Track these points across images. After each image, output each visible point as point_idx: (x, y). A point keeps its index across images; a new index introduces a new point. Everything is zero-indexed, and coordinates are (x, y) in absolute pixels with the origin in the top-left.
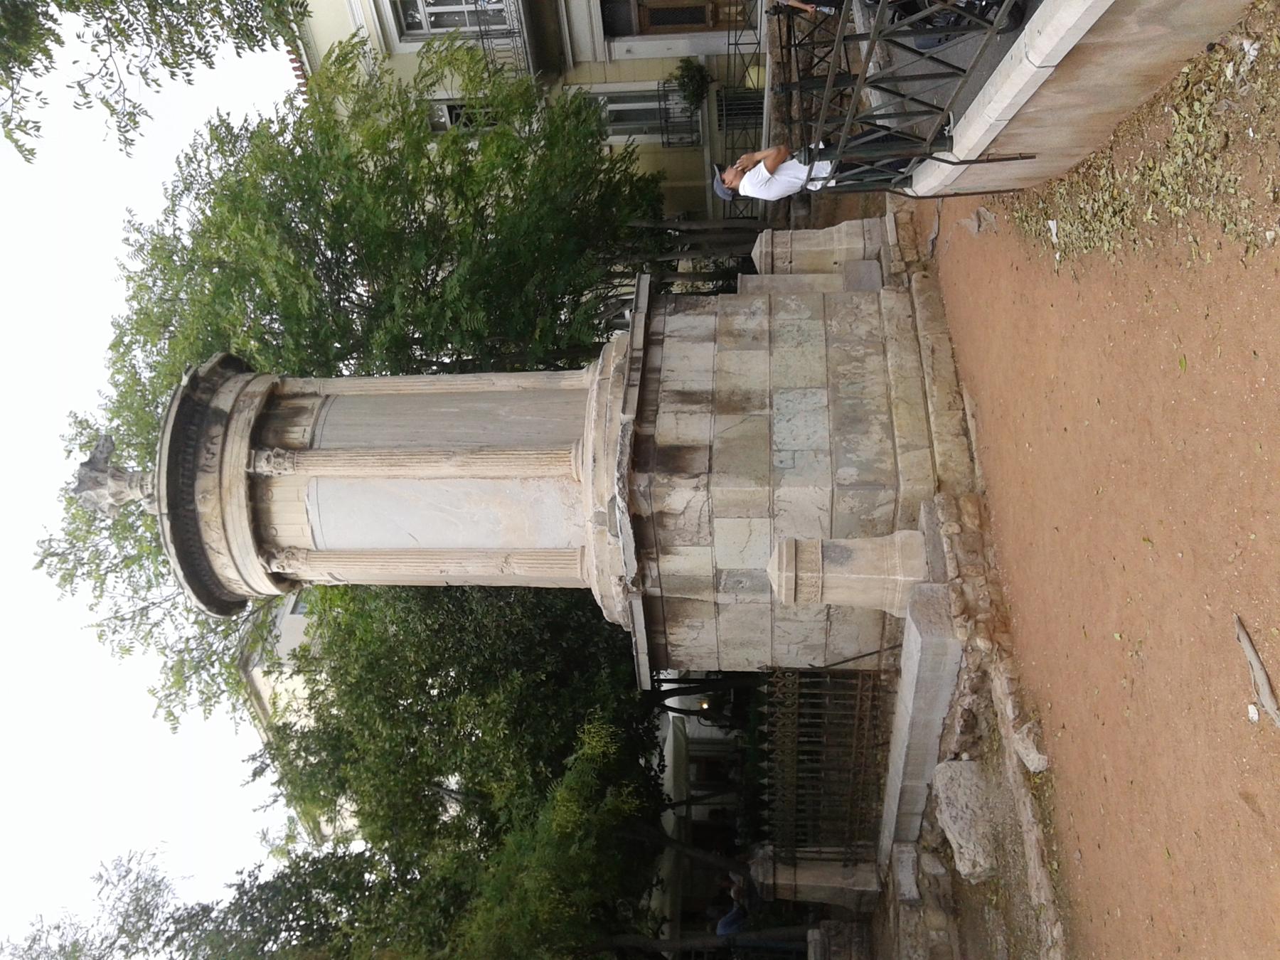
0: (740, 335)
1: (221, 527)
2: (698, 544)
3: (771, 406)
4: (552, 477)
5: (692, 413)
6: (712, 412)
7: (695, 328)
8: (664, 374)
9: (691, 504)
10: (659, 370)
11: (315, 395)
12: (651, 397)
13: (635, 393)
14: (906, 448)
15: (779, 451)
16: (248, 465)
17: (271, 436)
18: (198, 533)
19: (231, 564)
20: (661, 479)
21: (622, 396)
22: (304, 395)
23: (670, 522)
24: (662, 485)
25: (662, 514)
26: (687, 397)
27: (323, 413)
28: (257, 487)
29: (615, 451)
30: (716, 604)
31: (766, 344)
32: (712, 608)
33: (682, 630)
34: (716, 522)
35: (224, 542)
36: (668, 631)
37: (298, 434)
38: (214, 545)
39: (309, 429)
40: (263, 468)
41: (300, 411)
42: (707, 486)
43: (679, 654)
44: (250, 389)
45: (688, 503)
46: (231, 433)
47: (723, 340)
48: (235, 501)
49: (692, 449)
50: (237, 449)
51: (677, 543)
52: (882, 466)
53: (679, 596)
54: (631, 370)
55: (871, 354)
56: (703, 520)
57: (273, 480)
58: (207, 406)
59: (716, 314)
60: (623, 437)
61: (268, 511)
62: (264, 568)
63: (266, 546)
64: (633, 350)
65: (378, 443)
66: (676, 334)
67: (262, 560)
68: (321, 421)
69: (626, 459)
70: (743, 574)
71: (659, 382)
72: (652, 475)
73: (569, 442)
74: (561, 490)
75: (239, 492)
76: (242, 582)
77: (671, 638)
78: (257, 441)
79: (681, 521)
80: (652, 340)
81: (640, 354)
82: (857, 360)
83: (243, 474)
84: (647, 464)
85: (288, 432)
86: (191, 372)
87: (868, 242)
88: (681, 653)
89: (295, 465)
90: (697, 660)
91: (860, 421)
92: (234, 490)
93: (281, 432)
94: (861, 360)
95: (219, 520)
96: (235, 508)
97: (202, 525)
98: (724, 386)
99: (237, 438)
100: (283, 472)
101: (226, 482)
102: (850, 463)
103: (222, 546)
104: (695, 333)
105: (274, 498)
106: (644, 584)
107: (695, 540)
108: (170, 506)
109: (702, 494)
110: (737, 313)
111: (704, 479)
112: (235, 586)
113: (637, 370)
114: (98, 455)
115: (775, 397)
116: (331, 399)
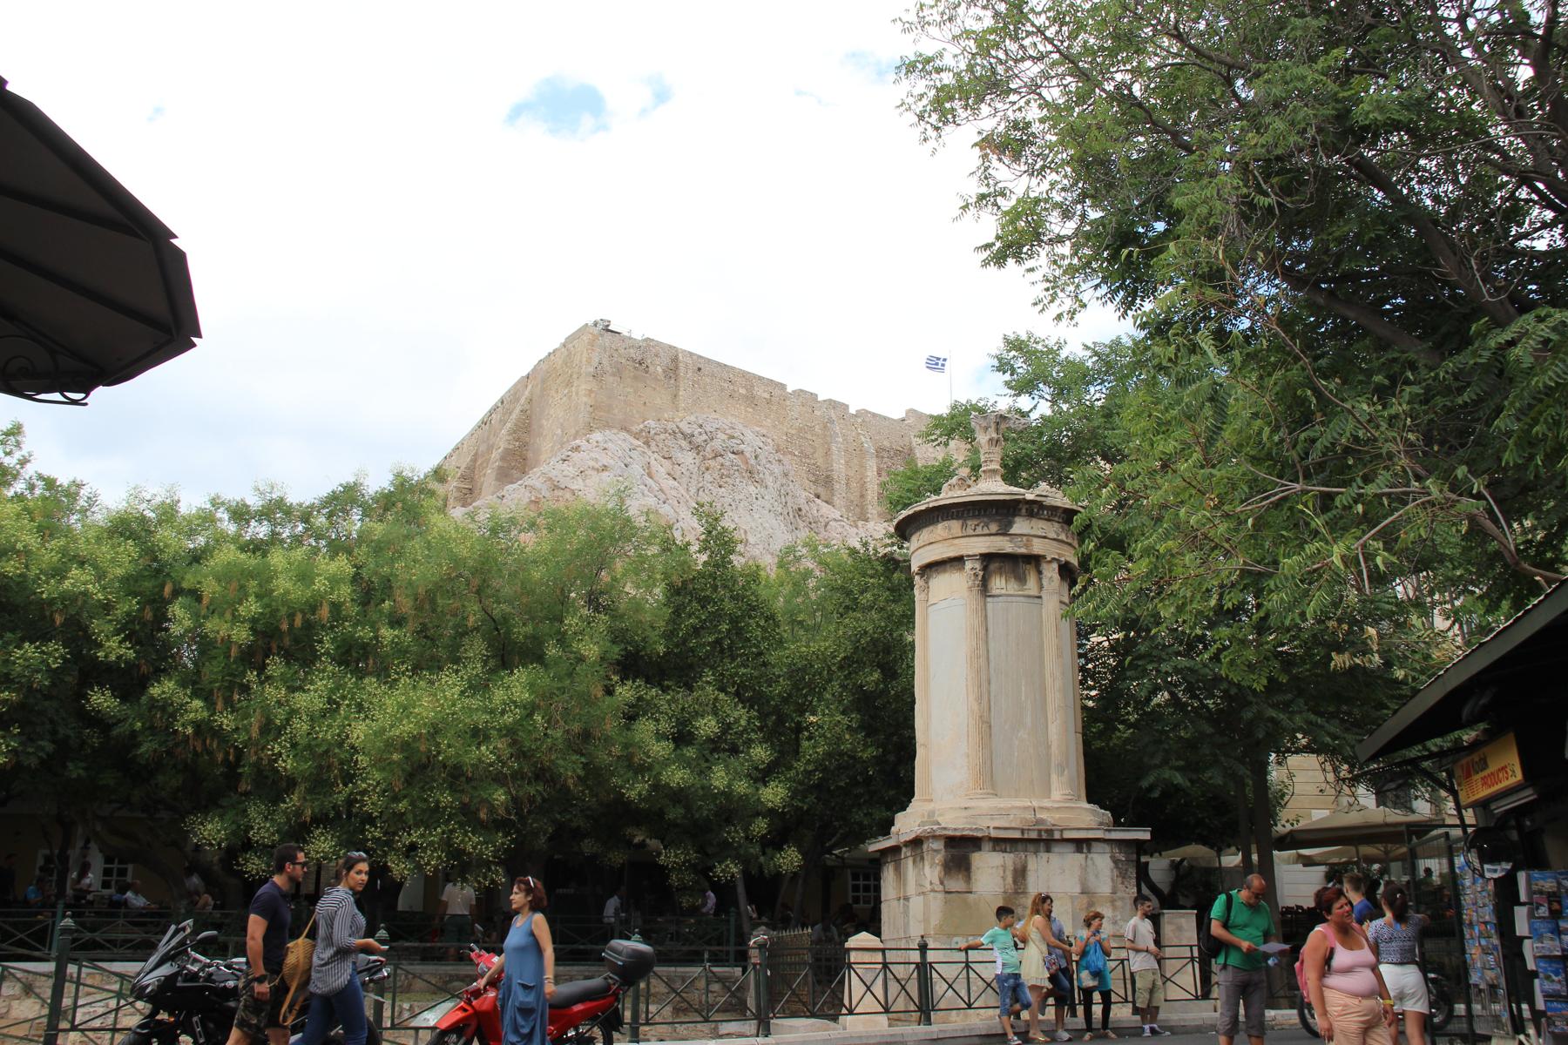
5: (1004, 878)
7: (1097, 876)
8: (1044, 856)
10: (1048, 850)
11: (1041, 587)
12: (1020, 846)
13: (1017, 835)
17: (997, 565)
20: (939, 858)
21: (1013, 825)
22: (1040, 579)
24: (933, 859)
25: (922, 859)
26: (1020, 874)
27: (1022, 599)
37: (998, 584)
39: (1003, 592)
40: (969, 565)
41: (1022, 580)
42: (933, 891)
44: (1035, 540)
47: (1085, 899)
49: (968, 878)
54: (1040, 831)
58: (1014, 515)
60: (971, 829)
61: (945, 571)
64: (1062, 831)
65: (992, 645)
66: (1089, 862)
68: (1010, 599)
69: (951, 833)
71: (1036, 852)
72: (943, 852)
73: (993, 786)
75: (951, 553)
78: (987, 558)
80: (1081, 845)
81: (1057, 836)
84: (952, 847)
86: (1039, 499)
89: (970, 588)
93: (1000, 571)
97: (931, 528)
101: (956, 541)
103: (921, 543)
104: (1091, 878)
108: (935, 508)
109: (929, 887)
111: (941, 888)
113: (1040, 835)
116: (1037, 601)
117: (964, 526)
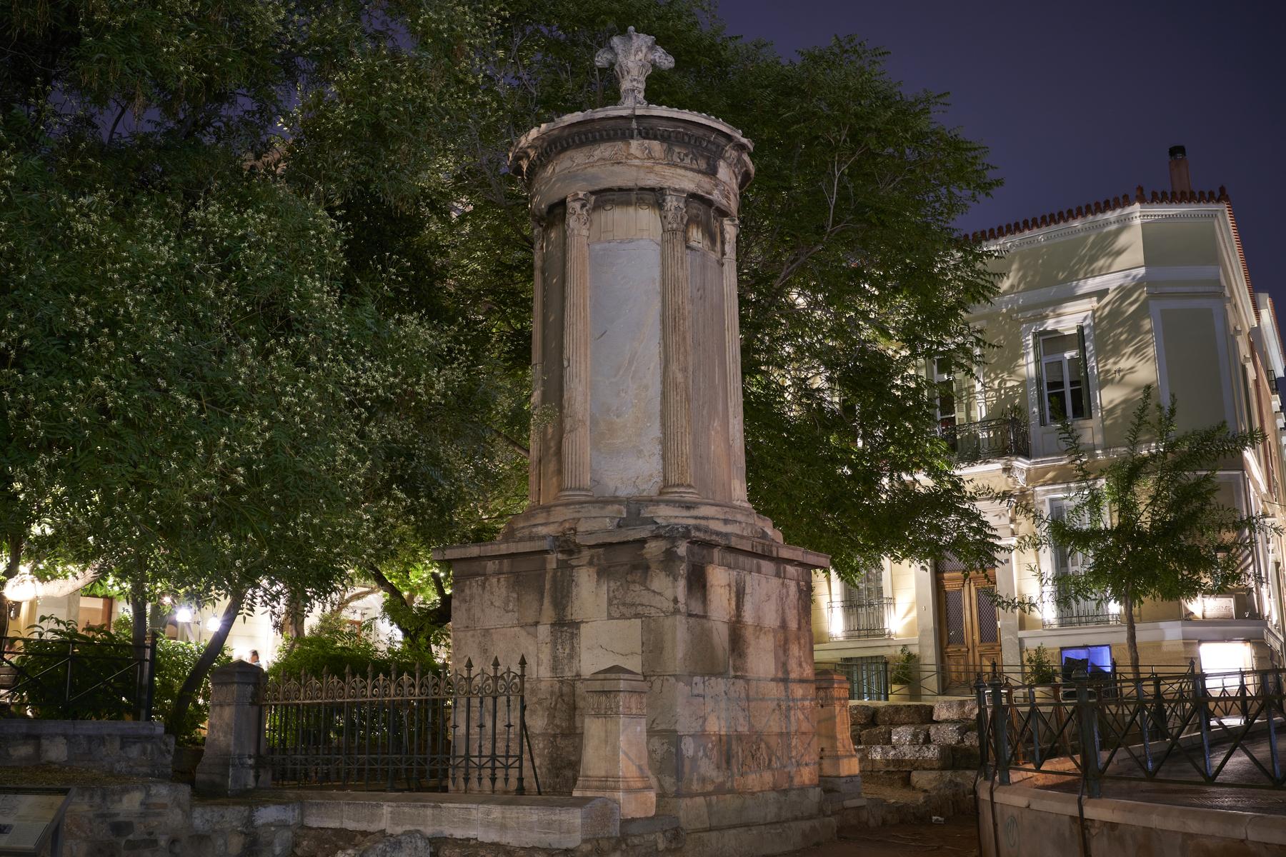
0: (786, 651)
2: (610, 603)
3: (736, 677)
4: (664, 468)
6: (730, 619)
9: (658, 598)
11: (723, 254)
12: (741, 559)
14: (709, 805)
15: (704, 682)
16: (675, 190)
18: (609, 139)
20: (683, 569)
23: (638, 575)
25: (648, 568)
26: (740, 595)
28: (654, 197)
29: (697, 528)
30: (536, 624)
31: (780, 675)
32: (530, 621)
33: (503, 590)
34: (638, 621)
36: (502, 578)
37: (696, 235)
38: (596, 153)
39: (700, 245)
40: (671, 202)
41: (713, 241)
43: (473, 588)
45: (660, 594)
47: (781, 636)
49: (704, 600)
50: (688, 181)
51: (612, 584)
52: (695, 782)
53: (547, 586)
55: (774, 775)
56: (640, 608)
57: (657, 212)
59: (799, 628)
61: (628, 203)
63: (593, 198)
67: (581, 195)
70: (573, 648)
74: (651, 475)
75: (651, 181)
77: (494, 580)
78: (693, 196)
79: (637, 587)
82: (770, 760)
85: (698, 228)
87: (844, 780)
88: (474, 590)
90: (464, 606)
91: (728, 762)
94: (769, 767)
97: (620, 144)
98: (749, 634)
101: (658, 168)
102: (696, 752)
105: (641, 211)
106: (561, 552)
107: (615, 602)
110: (800, 649)
113: (763, 550)
114: (658, 54)
115: (741, 681)
117: (669, 151)
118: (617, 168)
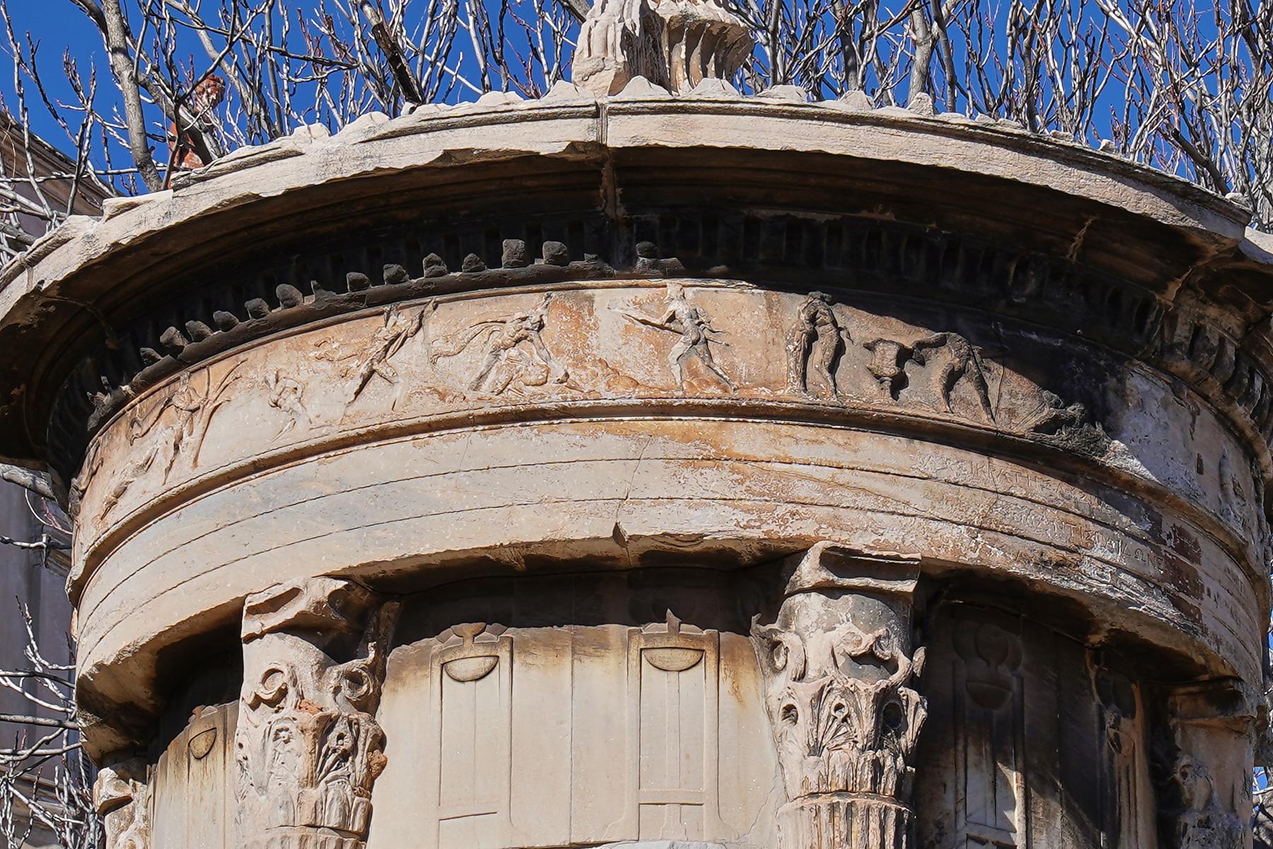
1: (513, 400)
19: (300, 436)
35: (431, 409)
38: (410, 356)
46: (998, 471)
48: (656, 480)
57: (748, 680)
62: (274, 604)
67: (318, 591)
76: (184, 475)
83: (793, 530)
92: (715, 480)
95: (552, 398)
96: (615, 480)
99: (978, 504)
100: (800, 733)
112: (161, 436)
118: (510, 439)
